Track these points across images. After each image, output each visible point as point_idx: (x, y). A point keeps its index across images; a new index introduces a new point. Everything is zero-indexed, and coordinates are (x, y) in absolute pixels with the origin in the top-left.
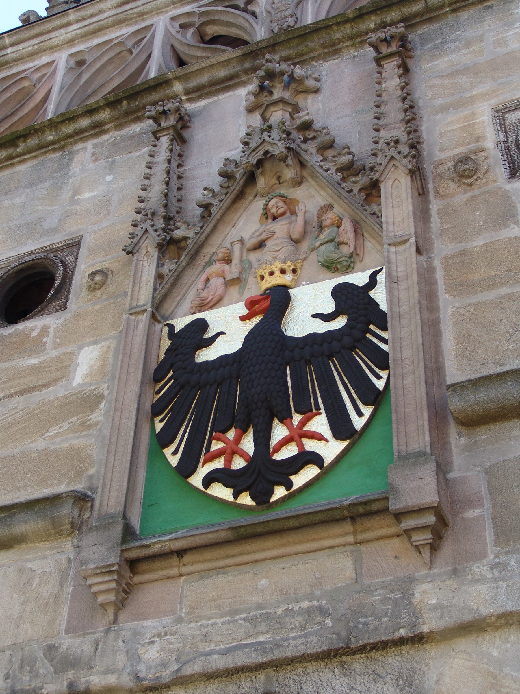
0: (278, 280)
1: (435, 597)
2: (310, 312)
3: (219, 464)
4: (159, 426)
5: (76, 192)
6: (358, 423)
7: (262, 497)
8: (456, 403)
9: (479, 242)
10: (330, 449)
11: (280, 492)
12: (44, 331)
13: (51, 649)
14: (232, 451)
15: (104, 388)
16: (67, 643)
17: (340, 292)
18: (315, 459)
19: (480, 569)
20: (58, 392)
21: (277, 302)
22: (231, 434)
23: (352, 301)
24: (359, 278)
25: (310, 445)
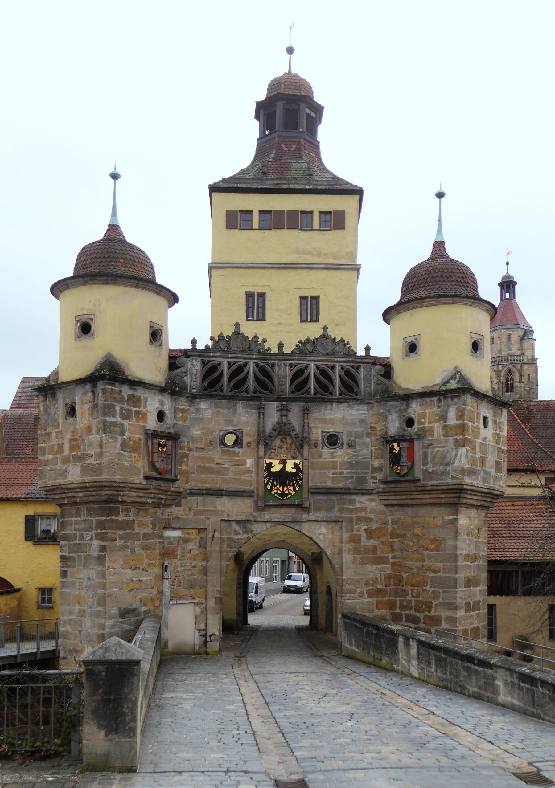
0: (284, 458)
1: (305, 516)
2: (290, 467)
3: (276, 491)
4: (266, 482)
5: (240, 416)
6: (297, 489)
7: (283, 499)
8: (311, 491)
9: (316, 460)
10: (293, 493)
11: (286, 498)
12: (239, 452)
13: (251, 514)
14: (278, 489)
15: (253, 469)
16: (254, 514)
17: (295, 464)
18: (291, 494)
19: (311, 514)
20: (243, 467)
21: (284, 463)
22: (278, 486)
23: (296, 466)
24: (298, 462)
25: (290, 492)
